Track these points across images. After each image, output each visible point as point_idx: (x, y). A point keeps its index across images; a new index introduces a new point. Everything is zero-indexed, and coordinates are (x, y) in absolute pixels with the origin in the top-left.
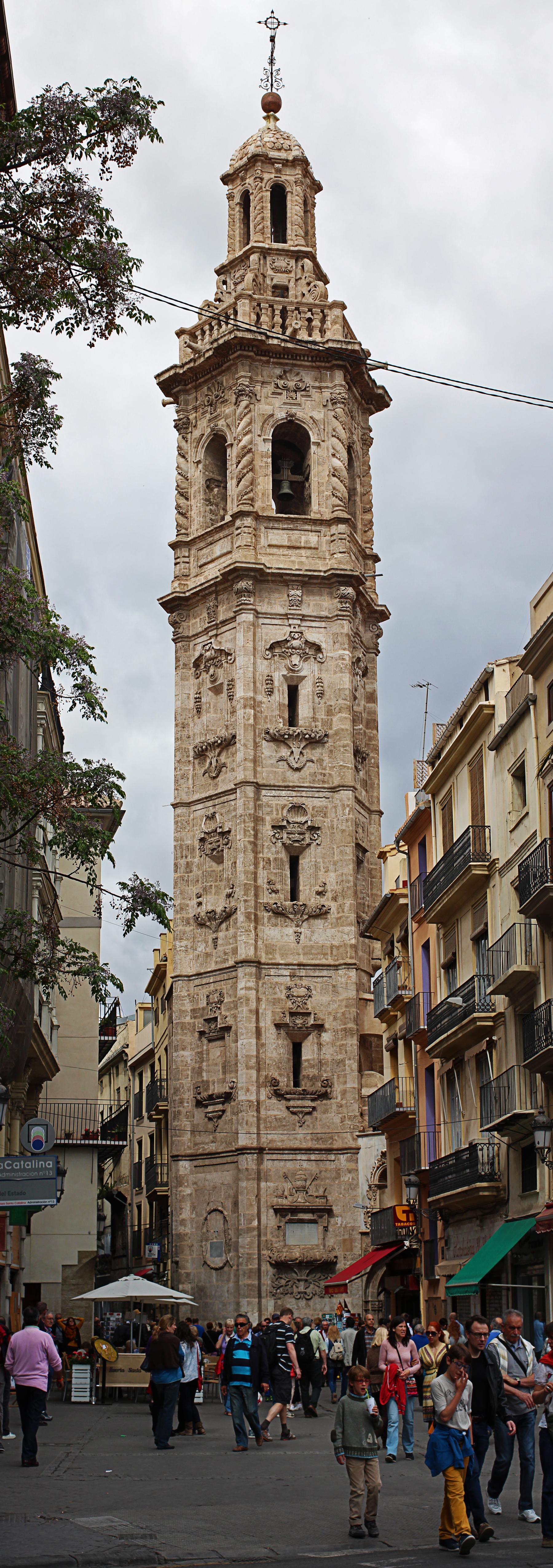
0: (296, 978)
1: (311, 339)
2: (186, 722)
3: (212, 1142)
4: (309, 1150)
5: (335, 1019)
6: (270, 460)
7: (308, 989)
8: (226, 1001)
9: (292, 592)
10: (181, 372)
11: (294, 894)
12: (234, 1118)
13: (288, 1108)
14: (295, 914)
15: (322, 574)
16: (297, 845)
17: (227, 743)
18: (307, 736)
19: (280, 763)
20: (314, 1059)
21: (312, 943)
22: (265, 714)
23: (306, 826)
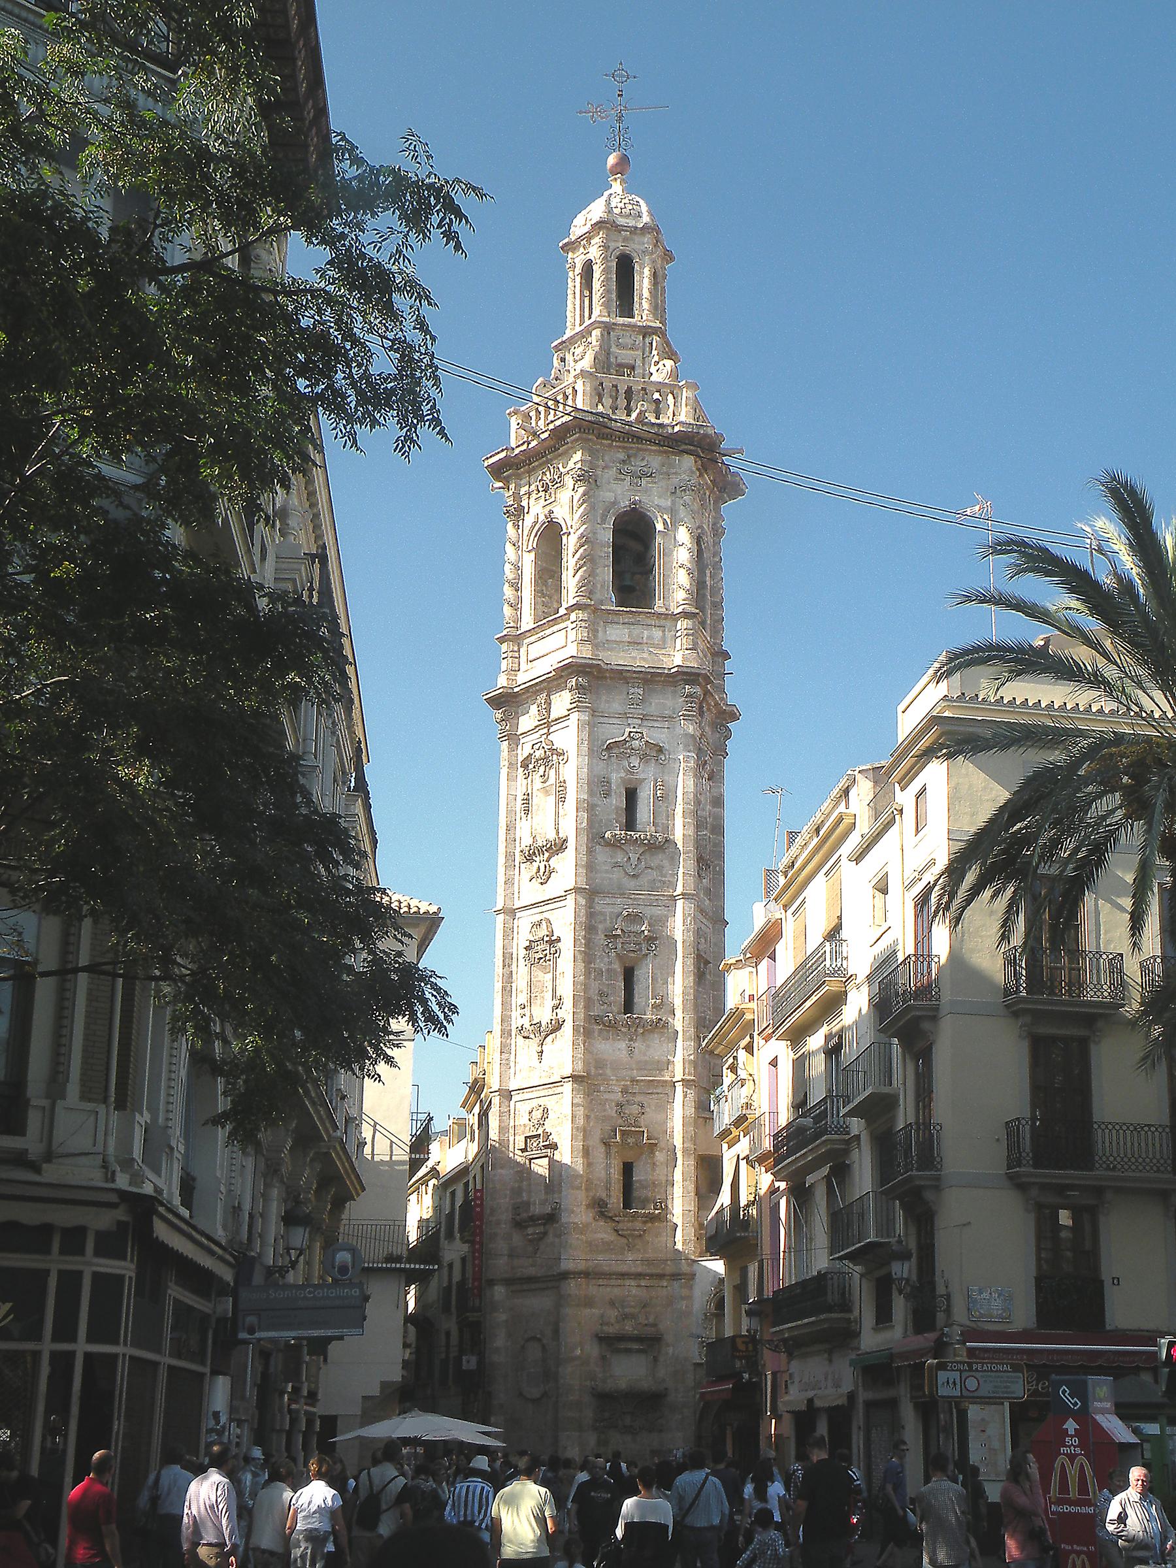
1: (658, 421)
3: (532, 1266)
4: (639, 1276)
9: (632, 691)
11: (628, 1006)
12: (557, 1240)
13: (617, 1231)
17: (558, 847)
18: (646, 842)
19: (615, 869)
21: (646, 1058)
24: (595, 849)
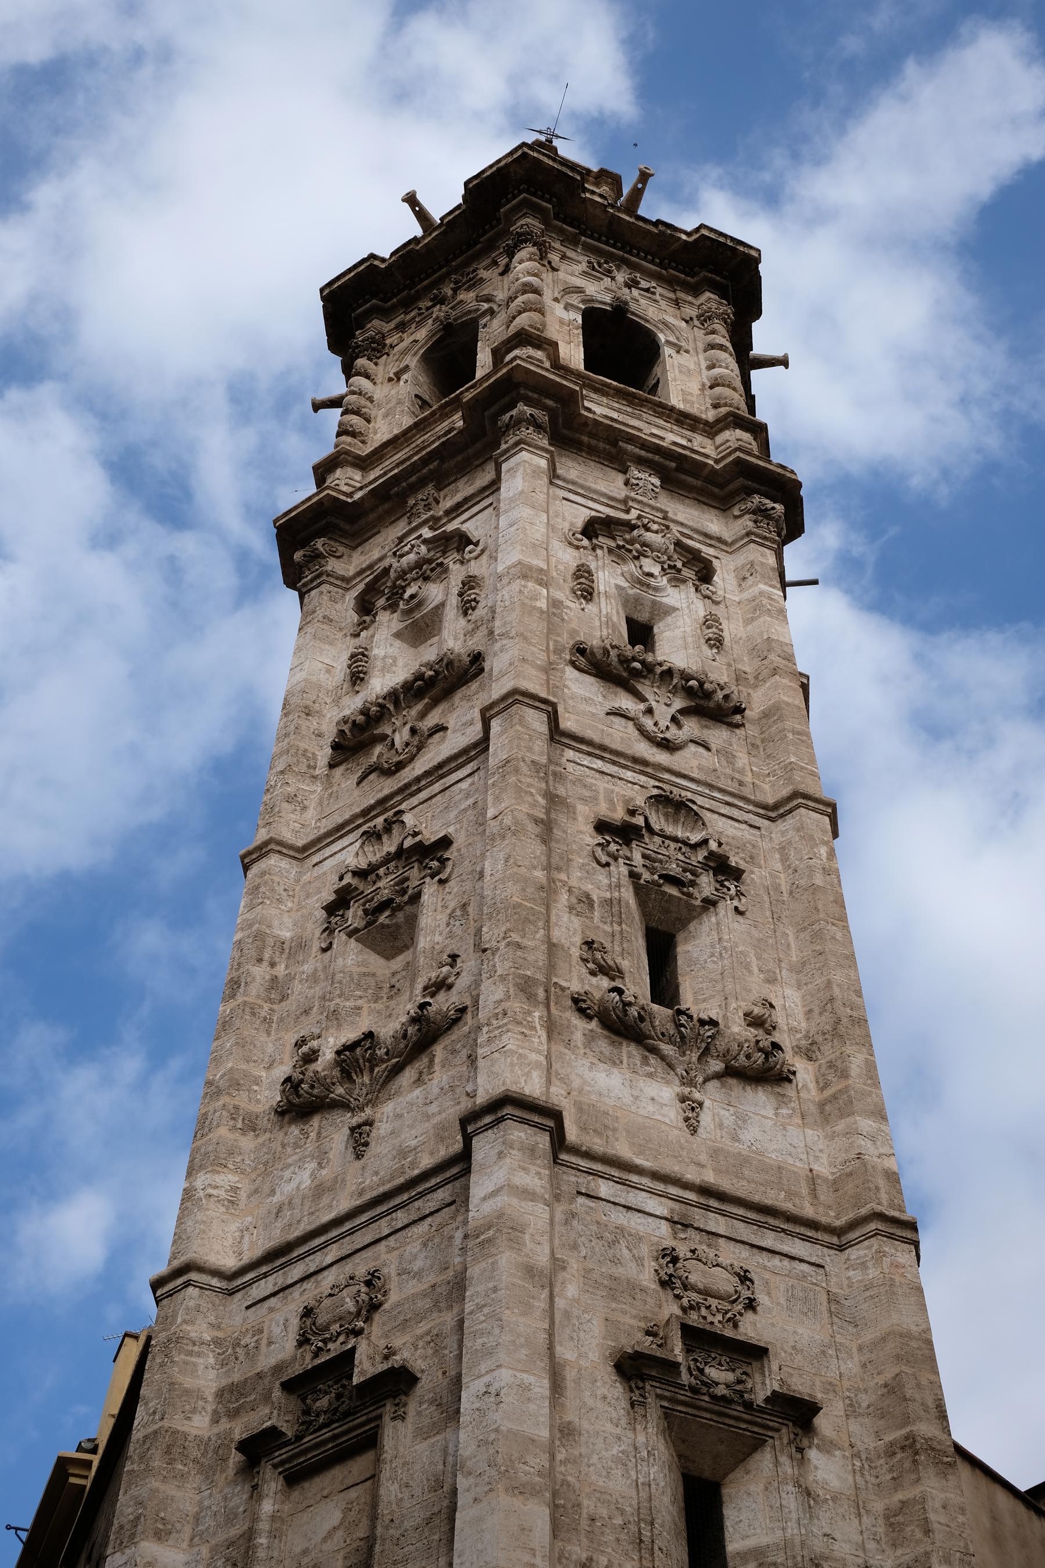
0: (691, 1232)
2: (317, 706)
5: (852, 1410)
6: (580, 331)
7: (744, 1278)
8: (394, 1297)
10: (383, 266)
14: (682, 1042)
15: (711, 462)
16: (673, 891)
18: (693, 683)
20: (787, 1545)
21: (742, 1148)
22: (574, 625)
23: (701, 855)
24: (563, 672)
